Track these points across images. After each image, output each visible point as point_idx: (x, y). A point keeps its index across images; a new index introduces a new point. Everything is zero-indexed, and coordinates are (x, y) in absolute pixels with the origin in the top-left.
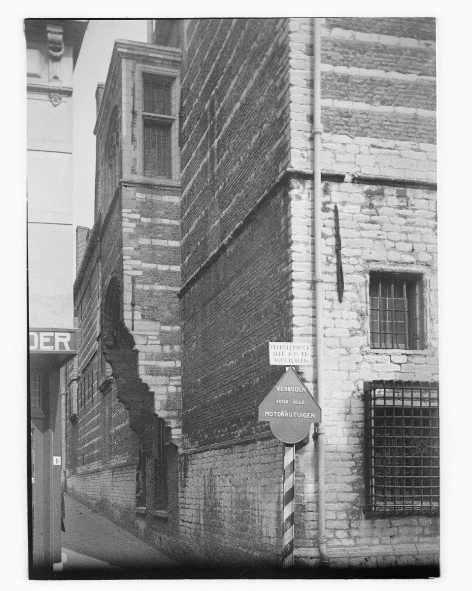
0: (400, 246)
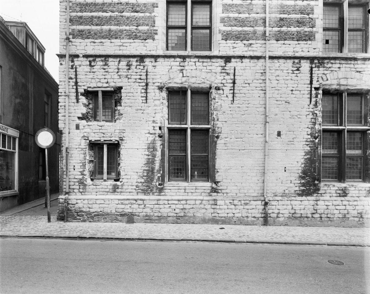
0: (103, 81)
